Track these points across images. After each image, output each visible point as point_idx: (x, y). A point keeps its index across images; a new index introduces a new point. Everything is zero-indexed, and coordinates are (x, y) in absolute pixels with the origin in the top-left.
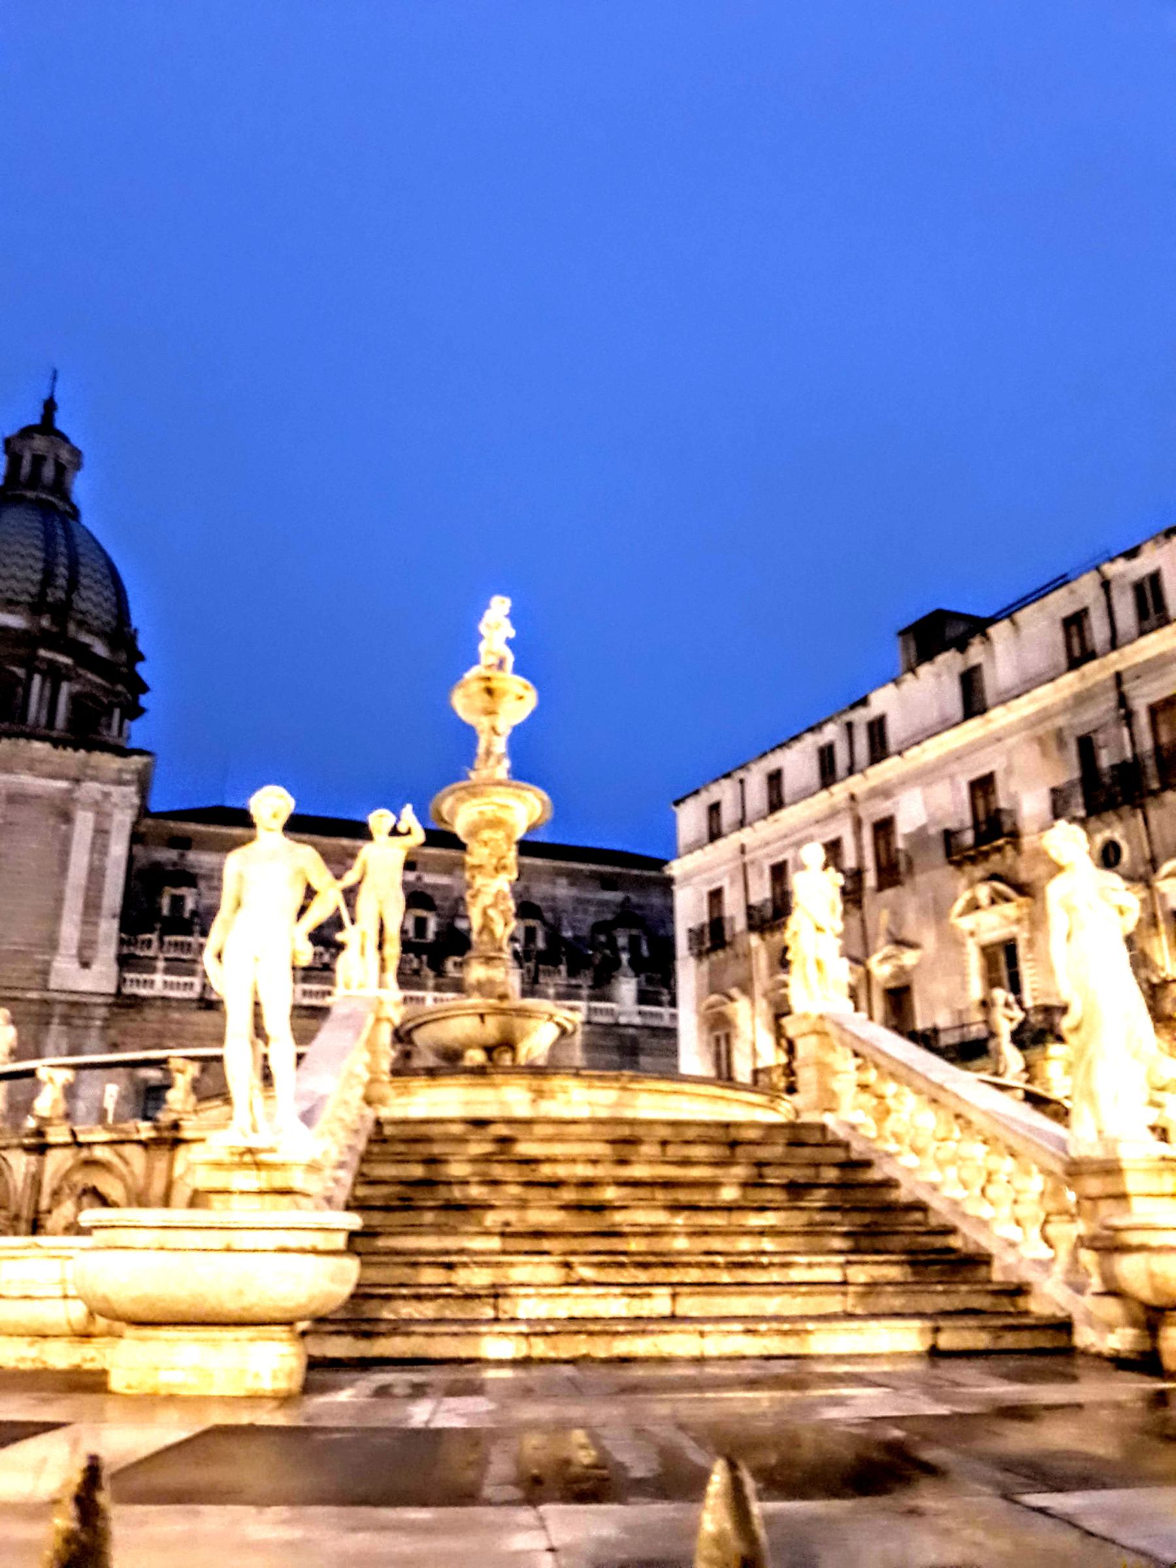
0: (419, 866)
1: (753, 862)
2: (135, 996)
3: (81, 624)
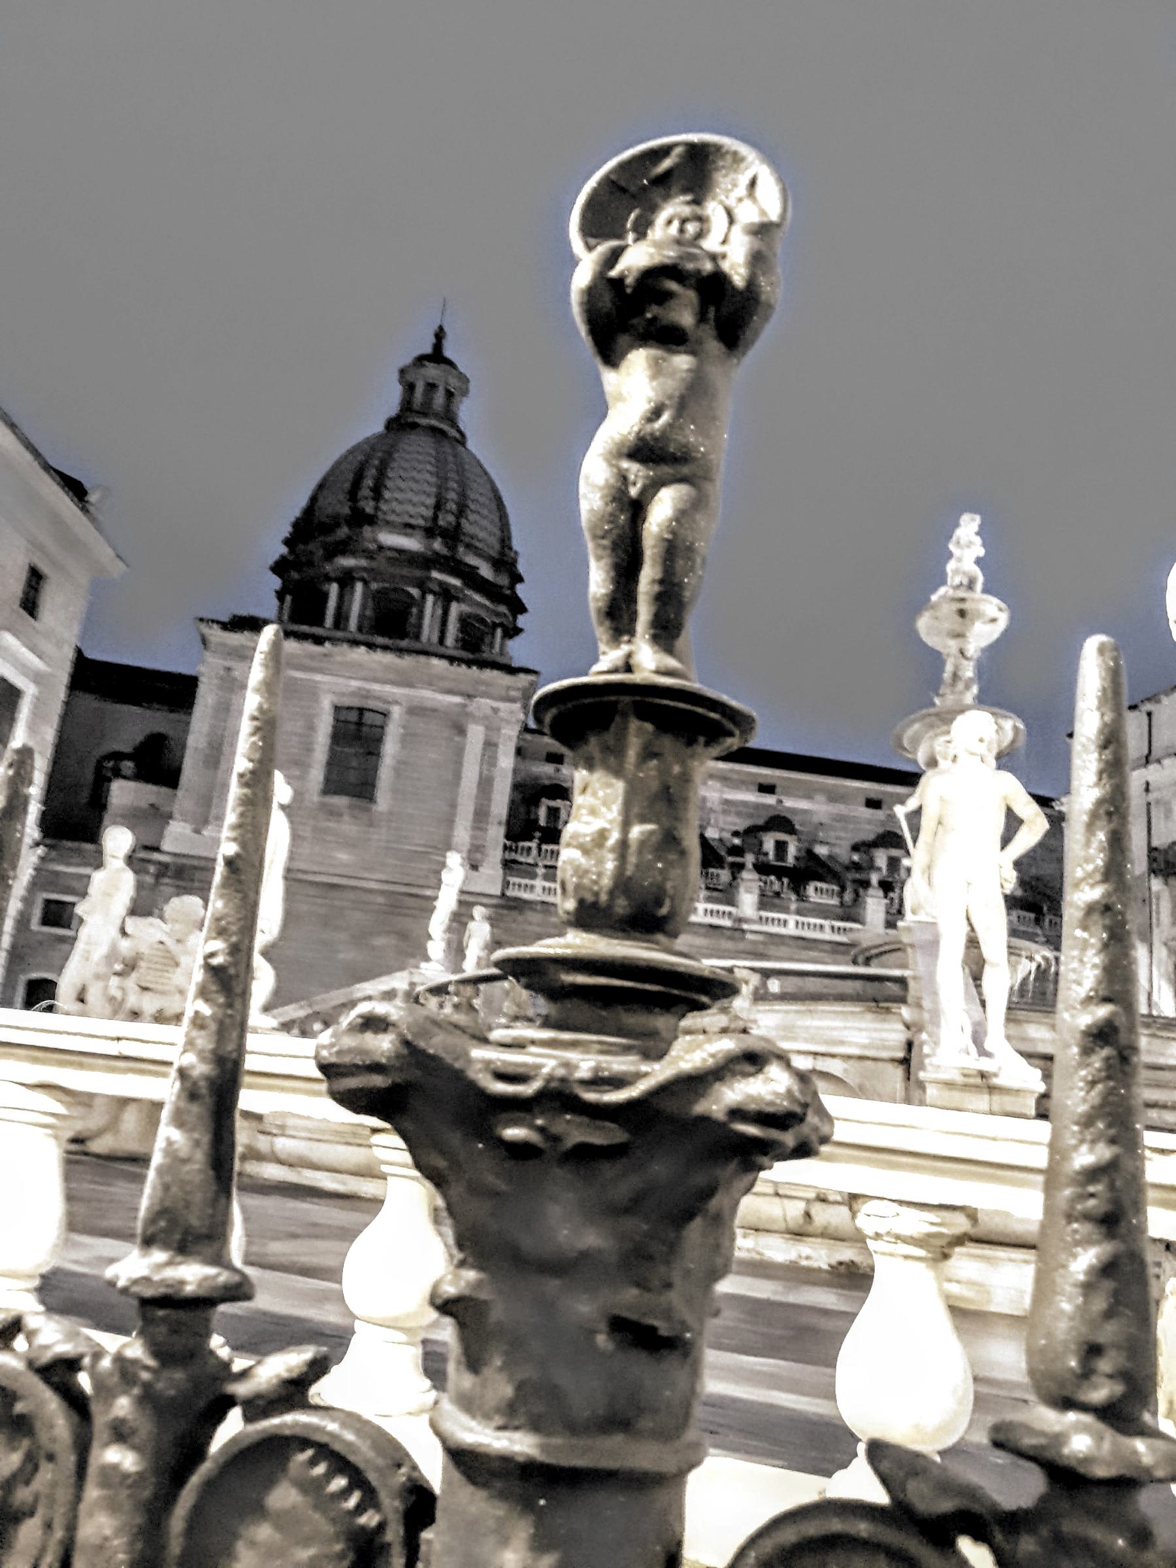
0: (778, 790)
1: (1158, 802)
2: (516, 899)
3: (468, 546)
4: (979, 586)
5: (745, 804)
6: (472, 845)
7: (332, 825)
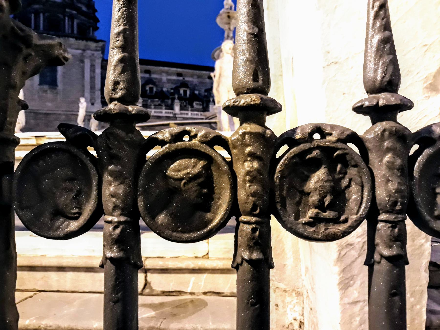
5: (174, 80)
7: (44, 94)
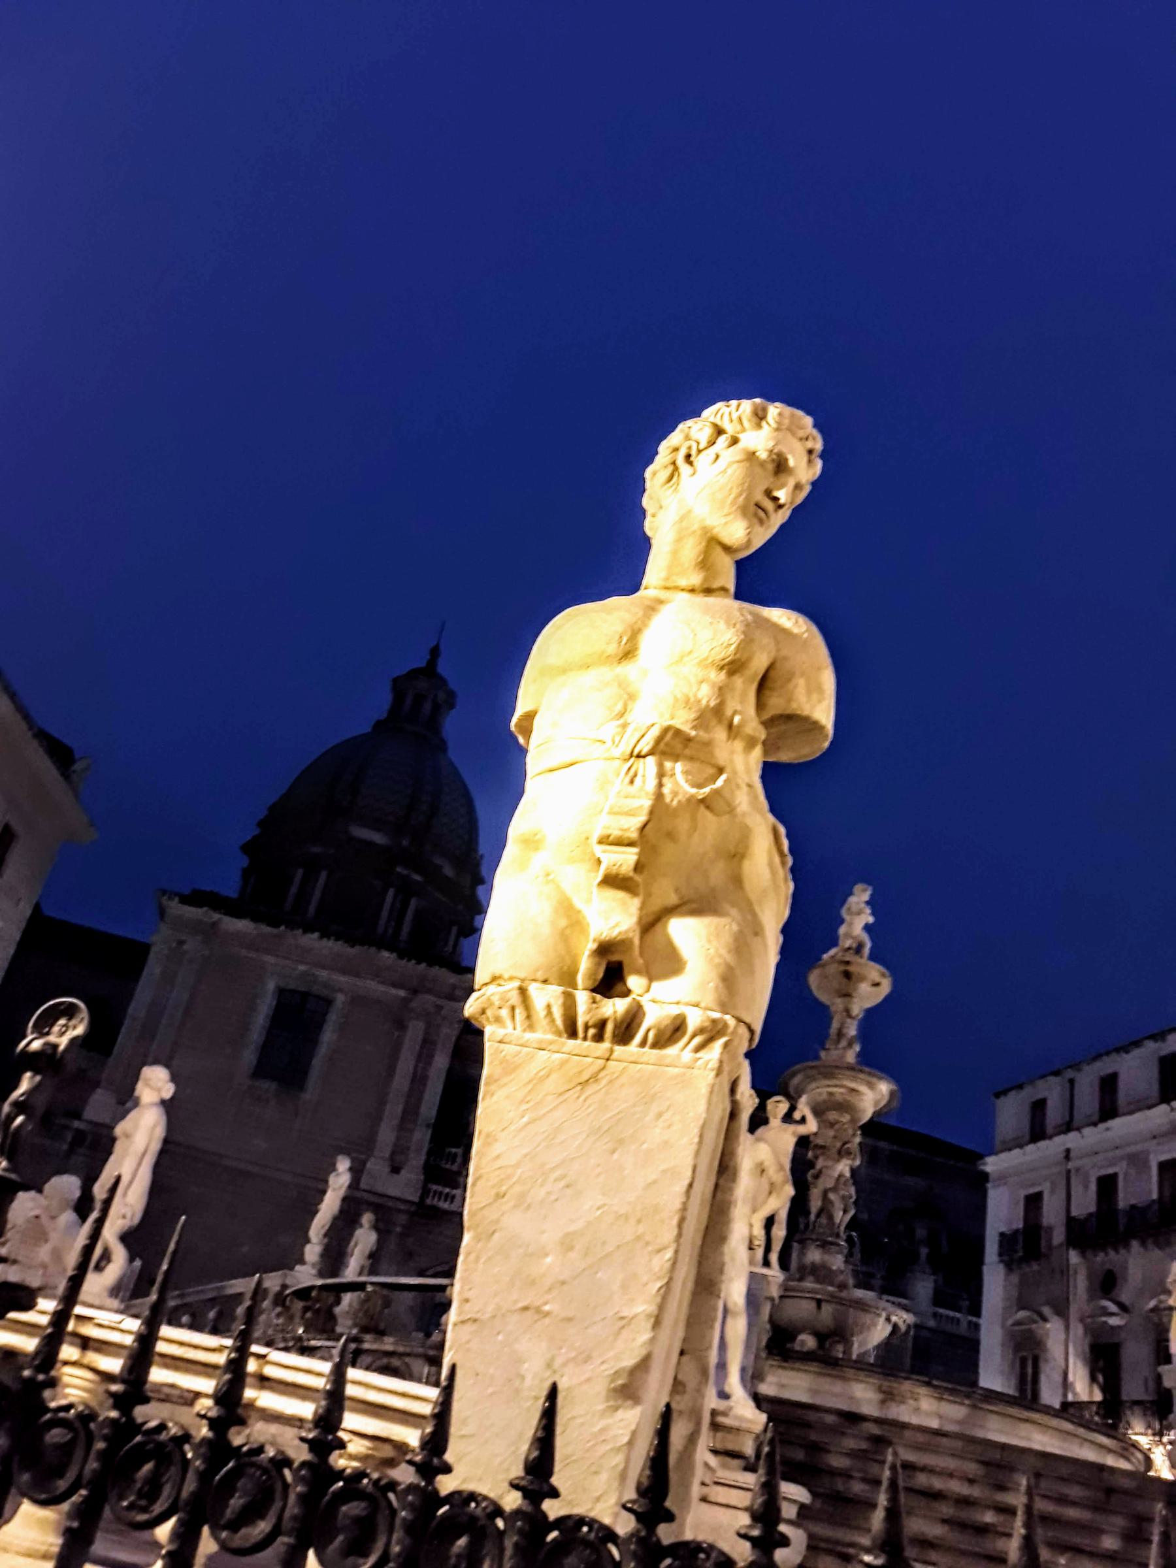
1: (1078, 1170)
4: (867, 950)
6: (395, 1145)
